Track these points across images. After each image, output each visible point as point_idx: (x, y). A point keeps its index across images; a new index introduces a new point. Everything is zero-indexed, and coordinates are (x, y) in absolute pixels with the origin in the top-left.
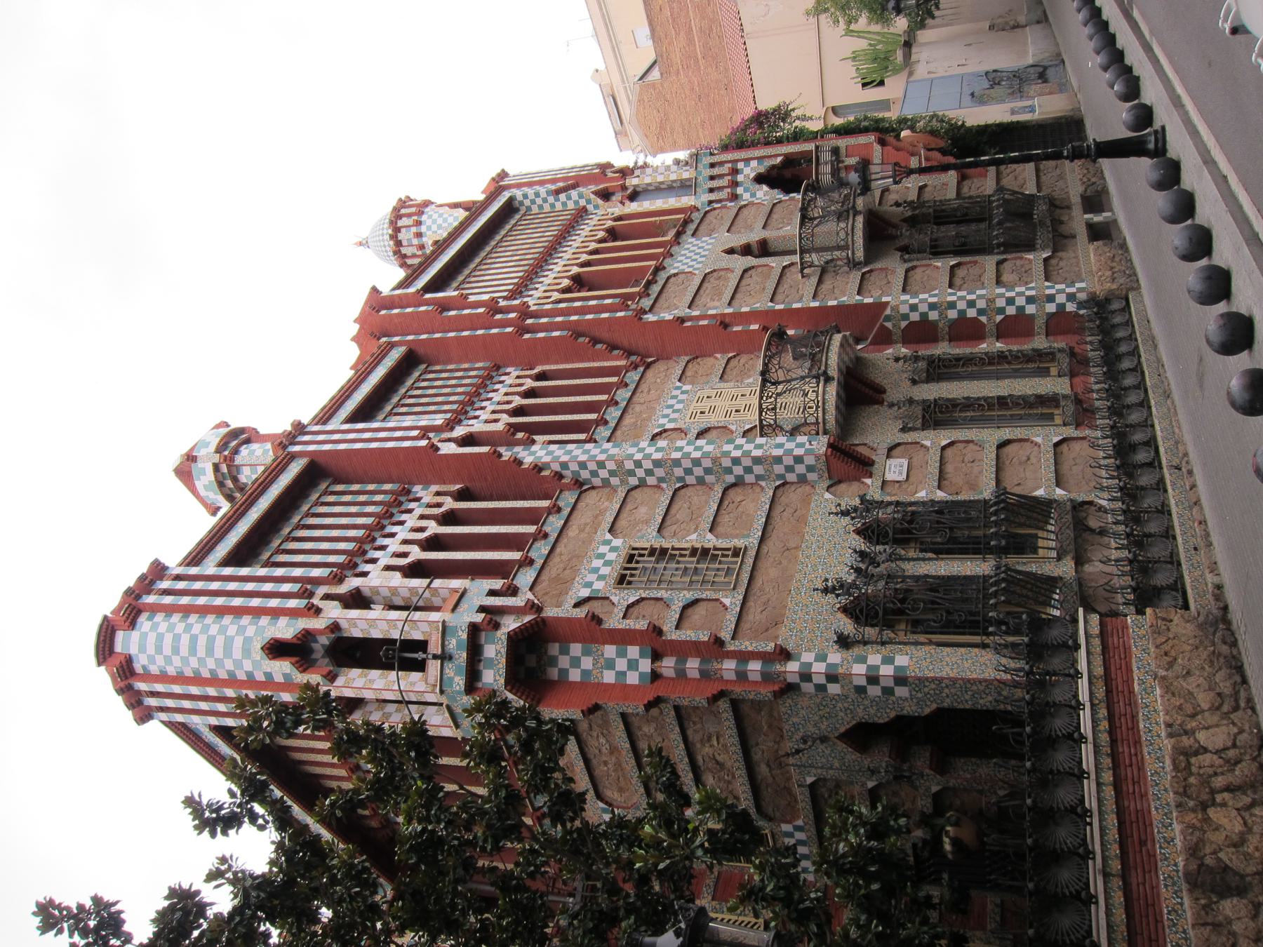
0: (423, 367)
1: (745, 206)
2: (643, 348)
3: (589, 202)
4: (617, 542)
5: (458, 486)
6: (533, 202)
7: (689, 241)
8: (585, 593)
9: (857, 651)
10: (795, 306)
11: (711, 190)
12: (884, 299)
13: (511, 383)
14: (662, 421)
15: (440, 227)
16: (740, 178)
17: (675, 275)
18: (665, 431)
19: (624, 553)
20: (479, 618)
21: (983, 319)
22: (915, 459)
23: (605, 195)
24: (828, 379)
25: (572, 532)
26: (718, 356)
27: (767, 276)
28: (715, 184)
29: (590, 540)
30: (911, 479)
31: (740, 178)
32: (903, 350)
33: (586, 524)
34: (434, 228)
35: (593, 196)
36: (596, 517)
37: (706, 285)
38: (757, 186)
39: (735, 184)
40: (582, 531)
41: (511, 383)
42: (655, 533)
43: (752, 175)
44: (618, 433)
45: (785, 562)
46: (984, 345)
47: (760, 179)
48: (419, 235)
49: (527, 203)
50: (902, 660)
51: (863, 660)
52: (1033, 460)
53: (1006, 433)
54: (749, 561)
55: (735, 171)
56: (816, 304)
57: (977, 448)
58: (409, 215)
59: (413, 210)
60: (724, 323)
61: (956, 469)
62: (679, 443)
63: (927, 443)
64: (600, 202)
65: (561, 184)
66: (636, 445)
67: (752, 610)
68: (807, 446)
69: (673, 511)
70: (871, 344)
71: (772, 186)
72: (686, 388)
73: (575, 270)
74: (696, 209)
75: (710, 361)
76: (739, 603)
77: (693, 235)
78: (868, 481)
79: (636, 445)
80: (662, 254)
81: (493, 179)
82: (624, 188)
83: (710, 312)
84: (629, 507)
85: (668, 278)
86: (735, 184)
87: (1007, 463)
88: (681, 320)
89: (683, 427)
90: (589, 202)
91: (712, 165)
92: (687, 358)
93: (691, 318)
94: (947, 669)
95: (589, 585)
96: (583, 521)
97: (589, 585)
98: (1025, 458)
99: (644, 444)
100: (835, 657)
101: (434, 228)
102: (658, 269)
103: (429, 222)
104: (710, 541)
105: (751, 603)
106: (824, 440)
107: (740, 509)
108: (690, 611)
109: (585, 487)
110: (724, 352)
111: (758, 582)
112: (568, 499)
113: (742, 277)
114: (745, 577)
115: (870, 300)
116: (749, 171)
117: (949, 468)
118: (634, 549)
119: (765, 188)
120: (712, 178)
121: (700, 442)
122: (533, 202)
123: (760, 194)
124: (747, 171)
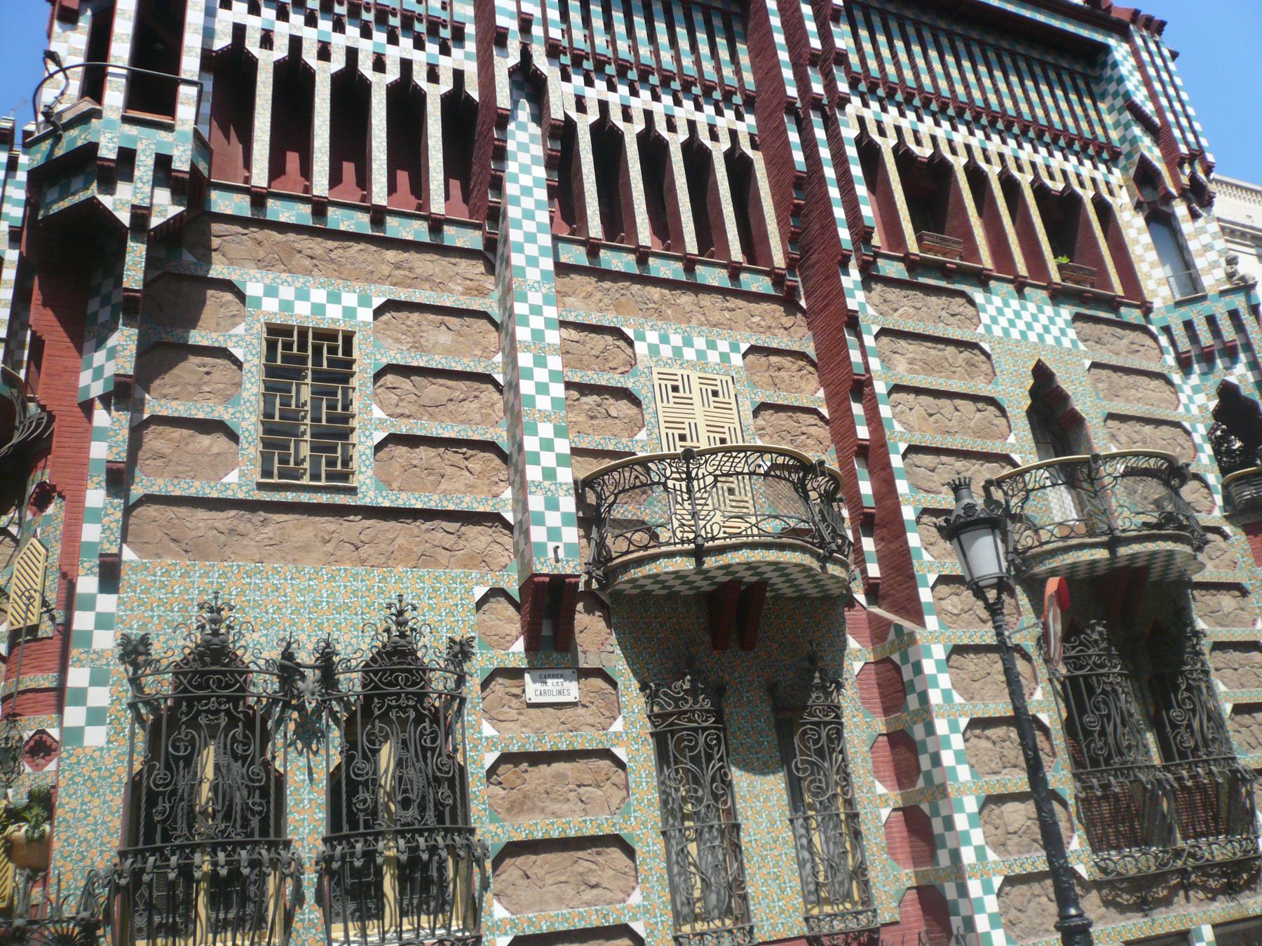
0: (735, 8)
1: (1169, 382)
2: (808, 281)
3: (1129, 156)
4: (366, 315)
5: (475, 95)
6: (1110, 79)
7: (1066, 312)
8: (253, 289)
9: (121, 671)
10: (902, 486)
11: (1188, 325)
12: (931, 621)
13: (728, 129)
14: (652, 337)
17: (972, 302)
18: (631, 343)
19: (342, 326)
20: (108, 151)
21: (921, 783)
22: (580, 711)
23: (1145, 176)
24: (699, 553)
26: (821, 393)
27: (979, 433)
29: (371, 277)
30: (532, 711)
32: (858, 666)
33: (411, 269)
35: (1136, 158)
36: (428, 279)
37: (951, 350)
38: (1213, 392)
39: (1207, 358)
40: (398, 266)
41: (728, 129)
45: (329, 547)
46: (880, 789)
47: (1227, 393)
49: (1108, 72)
50: (96, 736)
51: (98, 679)
52: (589, 895)
53: (650, 846)
54: (324, 498)
56: (908, 513)
57: (615, 802)
60: (860, 387)
61: (560, 777)
62: (555, 363)
63: (618, 726)
64: (1132, 172)
65: (1149, 108)
66: (547, 300)
67: (214, 514)
68: (551, 545)
70: (870, 614)
71: (1218, 414)
72: (737, 359)
73: (959, 162)
74: (1147, 309)
75: (814, 381)
76: (229, 494)
77: (1077, 318)
78: (519, 646)
79: (547, 300)
80: (1017, 276)
81: (1136, 13)
83: (874, 363)
84: (453, 321)
85: (962, 294)
86: (1207, 358)
87: (580, 854)
88: (852, 321)
89: (640, 366)
90: (1129, 156)
92: (811, 350)
93: (859, 336)
94: (74, 803)
95: (271, 291)
96: (417, 264)
98: (593, 881)
99: (551, 312)
100: (106, 641)
102: (981, 278)
104: (364, 439)
106: (572, 566)
107: (449, 470)
109: (489, 255)
110: (829, 400)
112: (472, 239)
113: (975, 398)
114: (290, 497)
115: (925, 595)
117: (558, 767)
118: (348, 338)
119: (1213, 404)
120: (1211, 320)
121: (558, 390)
122: (1110, 79)
123: (1200, 398)
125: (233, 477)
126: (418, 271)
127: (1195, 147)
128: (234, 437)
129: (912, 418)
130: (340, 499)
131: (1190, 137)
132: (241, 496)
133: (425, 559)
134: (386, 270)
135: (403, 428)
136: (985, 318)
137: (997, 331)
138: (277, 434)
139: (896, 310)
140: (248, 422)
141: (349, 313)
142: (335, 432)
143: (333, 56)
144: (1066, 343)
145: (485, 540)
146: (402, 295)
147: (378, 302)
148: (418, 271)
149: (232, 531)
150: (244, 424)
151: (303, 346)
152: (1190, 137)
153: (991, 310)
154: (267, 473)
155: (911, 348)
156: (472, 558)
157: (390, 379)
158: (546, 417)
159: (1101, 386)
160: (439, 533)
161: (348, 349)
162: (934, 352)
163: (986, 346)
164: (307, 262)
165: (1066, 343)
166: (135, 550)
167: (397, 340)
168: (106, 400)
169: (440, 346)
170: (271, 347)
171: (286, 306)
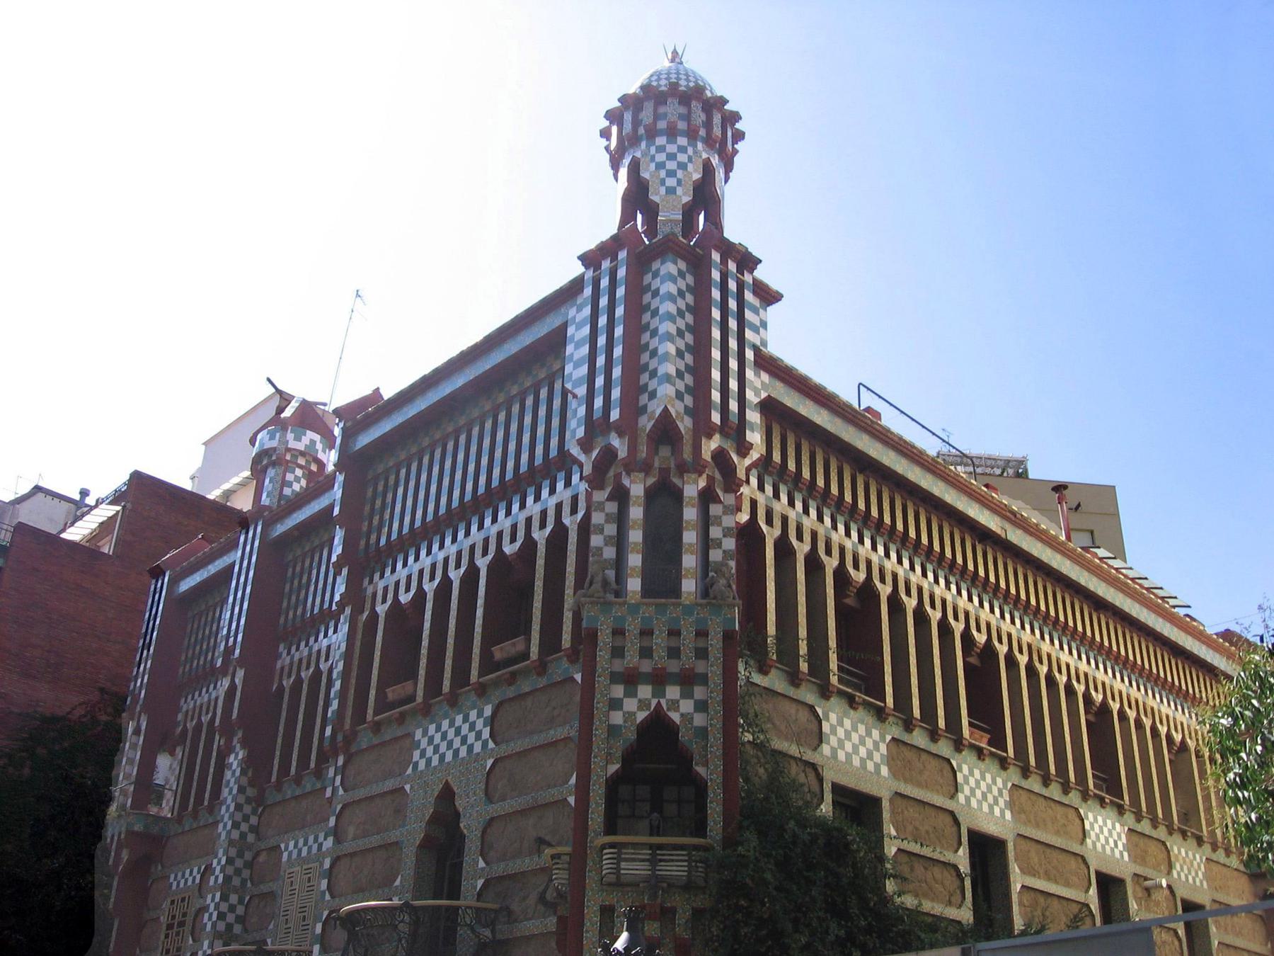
15: (661, 166)
16: (673, 692)
28: (660, 641)
31: (673, 692)
34: (661, 157)
43: (675, 717)
48: (652, 134)
55: (688, 680)
58: (708, 124)
59: (717, 131)
82: (683, 469)
86: (659, 680)
91: (702, 634)
101: (661, 157)
103: (672, 148)
116: (681, 707)
124: (687, 706)
127: (734, 419)
131: (733, 406)
152: (733, 406)
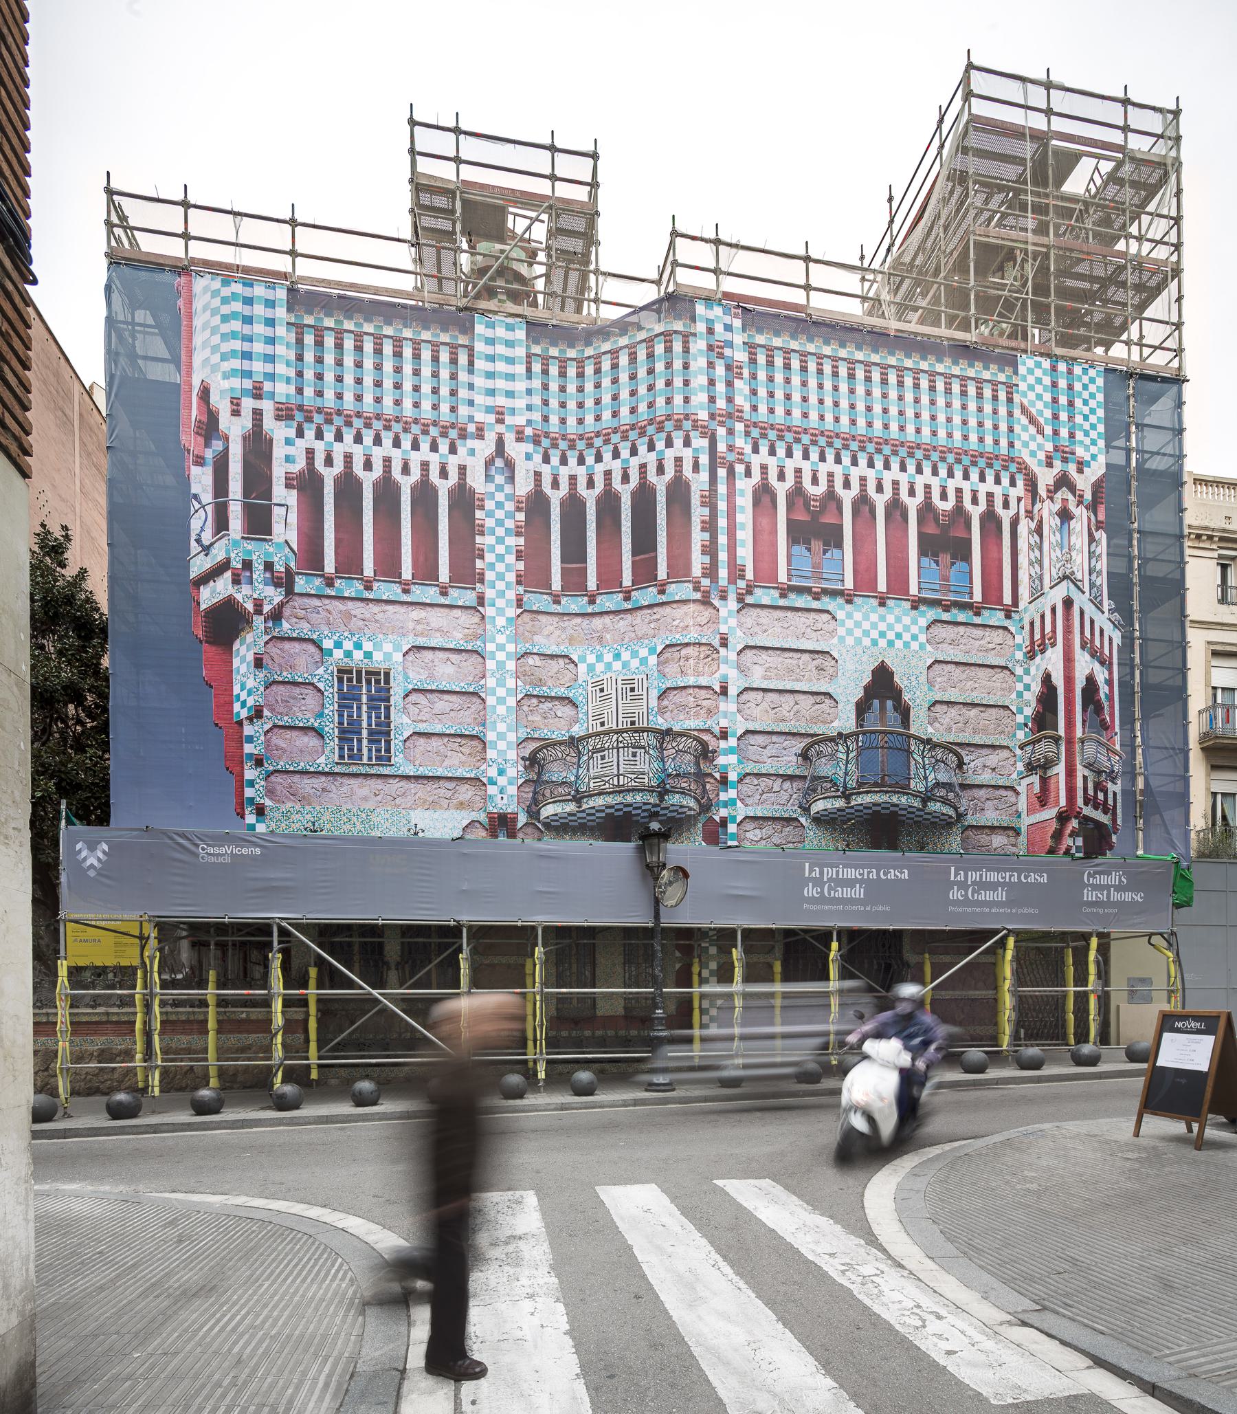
4: (398, 657)
19: (383, 667)
25: (417, 614)
37: (806, 657)
40: (418, 622)
42: (411, 687)
44: (579, 620)
45: (379, 798)
67: (313, 780)
69: (446, 697)
84: (454, 657)
97: (338, 645)
105: (323, 779)
107: (449, 753)
108: (311, 733)
111: (346, 781)
114: (354, 769)
118: (387, 674)
125: (322, 760)
126: (433, 625)
128: (321, 735)
129: (757, 712)
130: (386, 771)
132: (327, 770)
133: (433, 805)
134: (411, 625)
135: (422, 727)
136: (841, 631)
137: (850, 641)
138: (347, 733)
139: (766, 631)
140: (331, 728)
141: (388, 656)
142: (382, 732)
143: (374, 467)
144: (915, 646)
145: (470, 793)
146: (420, 641)
147: (405, 648)
148: (433, 625)
149: (324, 790)
150: (327, 729)
151: (359, 680)
153: (850, 624)
154: (341, 757)
155: (769, 659)
156: (462, 804)
157: (414, 697)
158: (503, 720)
159: (939, 680)
160: (443, 789)
161: (387, 682)
162: (790, 660)
163: (835, 655)
164: (361, 623)
165: (915, 646)
166: (271, 799)
167: (419, 673)
168: (250, 719)
169: (447, 673)
170: (340, 680)
171: (348, 654)
